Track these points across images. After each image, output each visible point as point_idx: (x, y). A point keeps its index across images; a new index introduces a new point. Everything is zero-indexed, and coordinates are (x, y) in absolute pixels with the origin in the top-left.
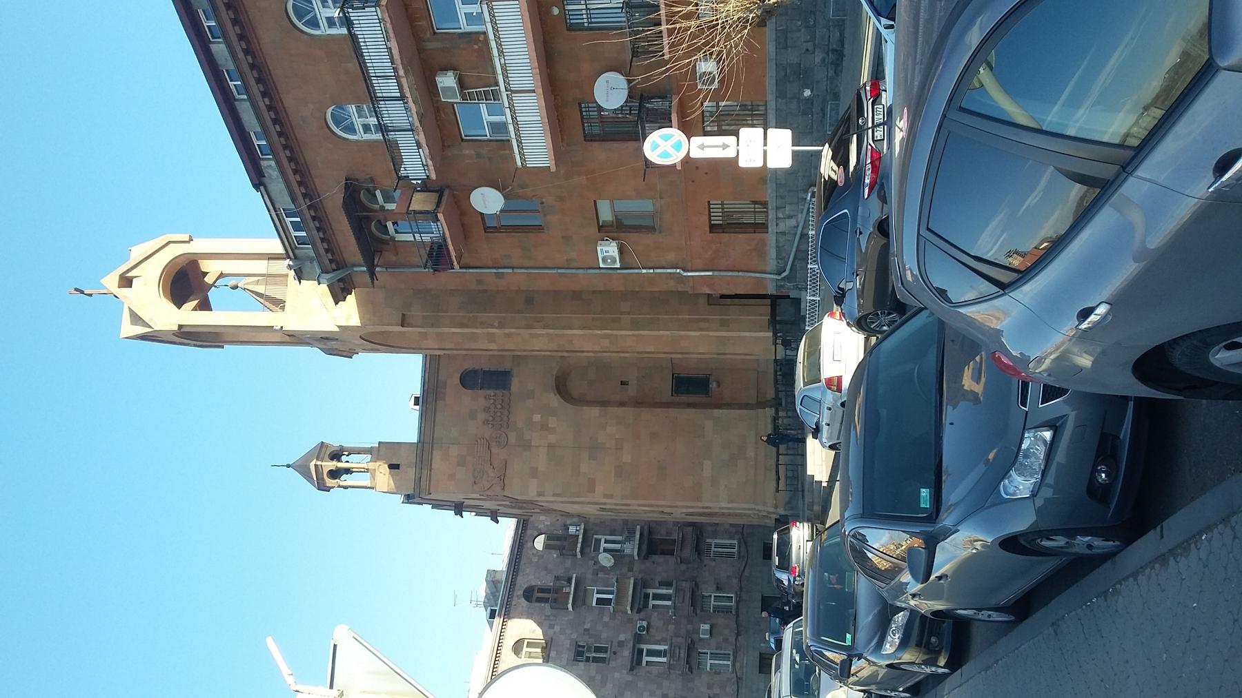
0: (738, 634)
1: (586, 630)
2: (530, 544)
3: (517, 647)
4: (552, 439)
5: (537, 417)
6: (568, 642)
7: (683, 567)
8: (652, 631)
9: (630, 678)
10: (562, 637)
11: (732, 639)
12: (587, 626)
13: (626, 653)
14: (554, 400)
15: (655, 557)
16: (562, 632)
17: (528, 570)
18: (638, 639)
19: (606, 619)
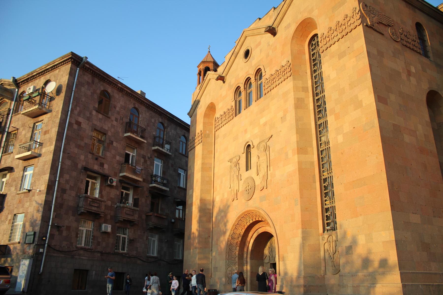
0: (102, 253)
1: (112, 143)
2: (160, 120)
3: (104, 93)
4: (404, 76)
5: (413, 70)
6: (107, 128)
7: (144, 217)
8: (108, 189)
9: (80, 166)
10: (110, 125)
11: (99, 249)
12: (115, 144)
13: (96, 168)
14: (426, 87)
15: (150, 198)
16: (113, 126)
17: (148, 114)
18: (105, 178)
19: (118, 158)
